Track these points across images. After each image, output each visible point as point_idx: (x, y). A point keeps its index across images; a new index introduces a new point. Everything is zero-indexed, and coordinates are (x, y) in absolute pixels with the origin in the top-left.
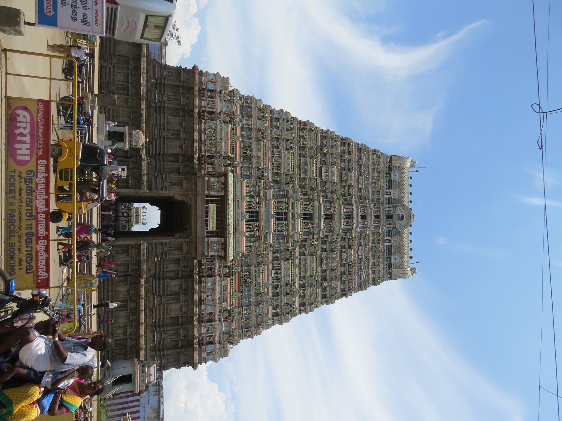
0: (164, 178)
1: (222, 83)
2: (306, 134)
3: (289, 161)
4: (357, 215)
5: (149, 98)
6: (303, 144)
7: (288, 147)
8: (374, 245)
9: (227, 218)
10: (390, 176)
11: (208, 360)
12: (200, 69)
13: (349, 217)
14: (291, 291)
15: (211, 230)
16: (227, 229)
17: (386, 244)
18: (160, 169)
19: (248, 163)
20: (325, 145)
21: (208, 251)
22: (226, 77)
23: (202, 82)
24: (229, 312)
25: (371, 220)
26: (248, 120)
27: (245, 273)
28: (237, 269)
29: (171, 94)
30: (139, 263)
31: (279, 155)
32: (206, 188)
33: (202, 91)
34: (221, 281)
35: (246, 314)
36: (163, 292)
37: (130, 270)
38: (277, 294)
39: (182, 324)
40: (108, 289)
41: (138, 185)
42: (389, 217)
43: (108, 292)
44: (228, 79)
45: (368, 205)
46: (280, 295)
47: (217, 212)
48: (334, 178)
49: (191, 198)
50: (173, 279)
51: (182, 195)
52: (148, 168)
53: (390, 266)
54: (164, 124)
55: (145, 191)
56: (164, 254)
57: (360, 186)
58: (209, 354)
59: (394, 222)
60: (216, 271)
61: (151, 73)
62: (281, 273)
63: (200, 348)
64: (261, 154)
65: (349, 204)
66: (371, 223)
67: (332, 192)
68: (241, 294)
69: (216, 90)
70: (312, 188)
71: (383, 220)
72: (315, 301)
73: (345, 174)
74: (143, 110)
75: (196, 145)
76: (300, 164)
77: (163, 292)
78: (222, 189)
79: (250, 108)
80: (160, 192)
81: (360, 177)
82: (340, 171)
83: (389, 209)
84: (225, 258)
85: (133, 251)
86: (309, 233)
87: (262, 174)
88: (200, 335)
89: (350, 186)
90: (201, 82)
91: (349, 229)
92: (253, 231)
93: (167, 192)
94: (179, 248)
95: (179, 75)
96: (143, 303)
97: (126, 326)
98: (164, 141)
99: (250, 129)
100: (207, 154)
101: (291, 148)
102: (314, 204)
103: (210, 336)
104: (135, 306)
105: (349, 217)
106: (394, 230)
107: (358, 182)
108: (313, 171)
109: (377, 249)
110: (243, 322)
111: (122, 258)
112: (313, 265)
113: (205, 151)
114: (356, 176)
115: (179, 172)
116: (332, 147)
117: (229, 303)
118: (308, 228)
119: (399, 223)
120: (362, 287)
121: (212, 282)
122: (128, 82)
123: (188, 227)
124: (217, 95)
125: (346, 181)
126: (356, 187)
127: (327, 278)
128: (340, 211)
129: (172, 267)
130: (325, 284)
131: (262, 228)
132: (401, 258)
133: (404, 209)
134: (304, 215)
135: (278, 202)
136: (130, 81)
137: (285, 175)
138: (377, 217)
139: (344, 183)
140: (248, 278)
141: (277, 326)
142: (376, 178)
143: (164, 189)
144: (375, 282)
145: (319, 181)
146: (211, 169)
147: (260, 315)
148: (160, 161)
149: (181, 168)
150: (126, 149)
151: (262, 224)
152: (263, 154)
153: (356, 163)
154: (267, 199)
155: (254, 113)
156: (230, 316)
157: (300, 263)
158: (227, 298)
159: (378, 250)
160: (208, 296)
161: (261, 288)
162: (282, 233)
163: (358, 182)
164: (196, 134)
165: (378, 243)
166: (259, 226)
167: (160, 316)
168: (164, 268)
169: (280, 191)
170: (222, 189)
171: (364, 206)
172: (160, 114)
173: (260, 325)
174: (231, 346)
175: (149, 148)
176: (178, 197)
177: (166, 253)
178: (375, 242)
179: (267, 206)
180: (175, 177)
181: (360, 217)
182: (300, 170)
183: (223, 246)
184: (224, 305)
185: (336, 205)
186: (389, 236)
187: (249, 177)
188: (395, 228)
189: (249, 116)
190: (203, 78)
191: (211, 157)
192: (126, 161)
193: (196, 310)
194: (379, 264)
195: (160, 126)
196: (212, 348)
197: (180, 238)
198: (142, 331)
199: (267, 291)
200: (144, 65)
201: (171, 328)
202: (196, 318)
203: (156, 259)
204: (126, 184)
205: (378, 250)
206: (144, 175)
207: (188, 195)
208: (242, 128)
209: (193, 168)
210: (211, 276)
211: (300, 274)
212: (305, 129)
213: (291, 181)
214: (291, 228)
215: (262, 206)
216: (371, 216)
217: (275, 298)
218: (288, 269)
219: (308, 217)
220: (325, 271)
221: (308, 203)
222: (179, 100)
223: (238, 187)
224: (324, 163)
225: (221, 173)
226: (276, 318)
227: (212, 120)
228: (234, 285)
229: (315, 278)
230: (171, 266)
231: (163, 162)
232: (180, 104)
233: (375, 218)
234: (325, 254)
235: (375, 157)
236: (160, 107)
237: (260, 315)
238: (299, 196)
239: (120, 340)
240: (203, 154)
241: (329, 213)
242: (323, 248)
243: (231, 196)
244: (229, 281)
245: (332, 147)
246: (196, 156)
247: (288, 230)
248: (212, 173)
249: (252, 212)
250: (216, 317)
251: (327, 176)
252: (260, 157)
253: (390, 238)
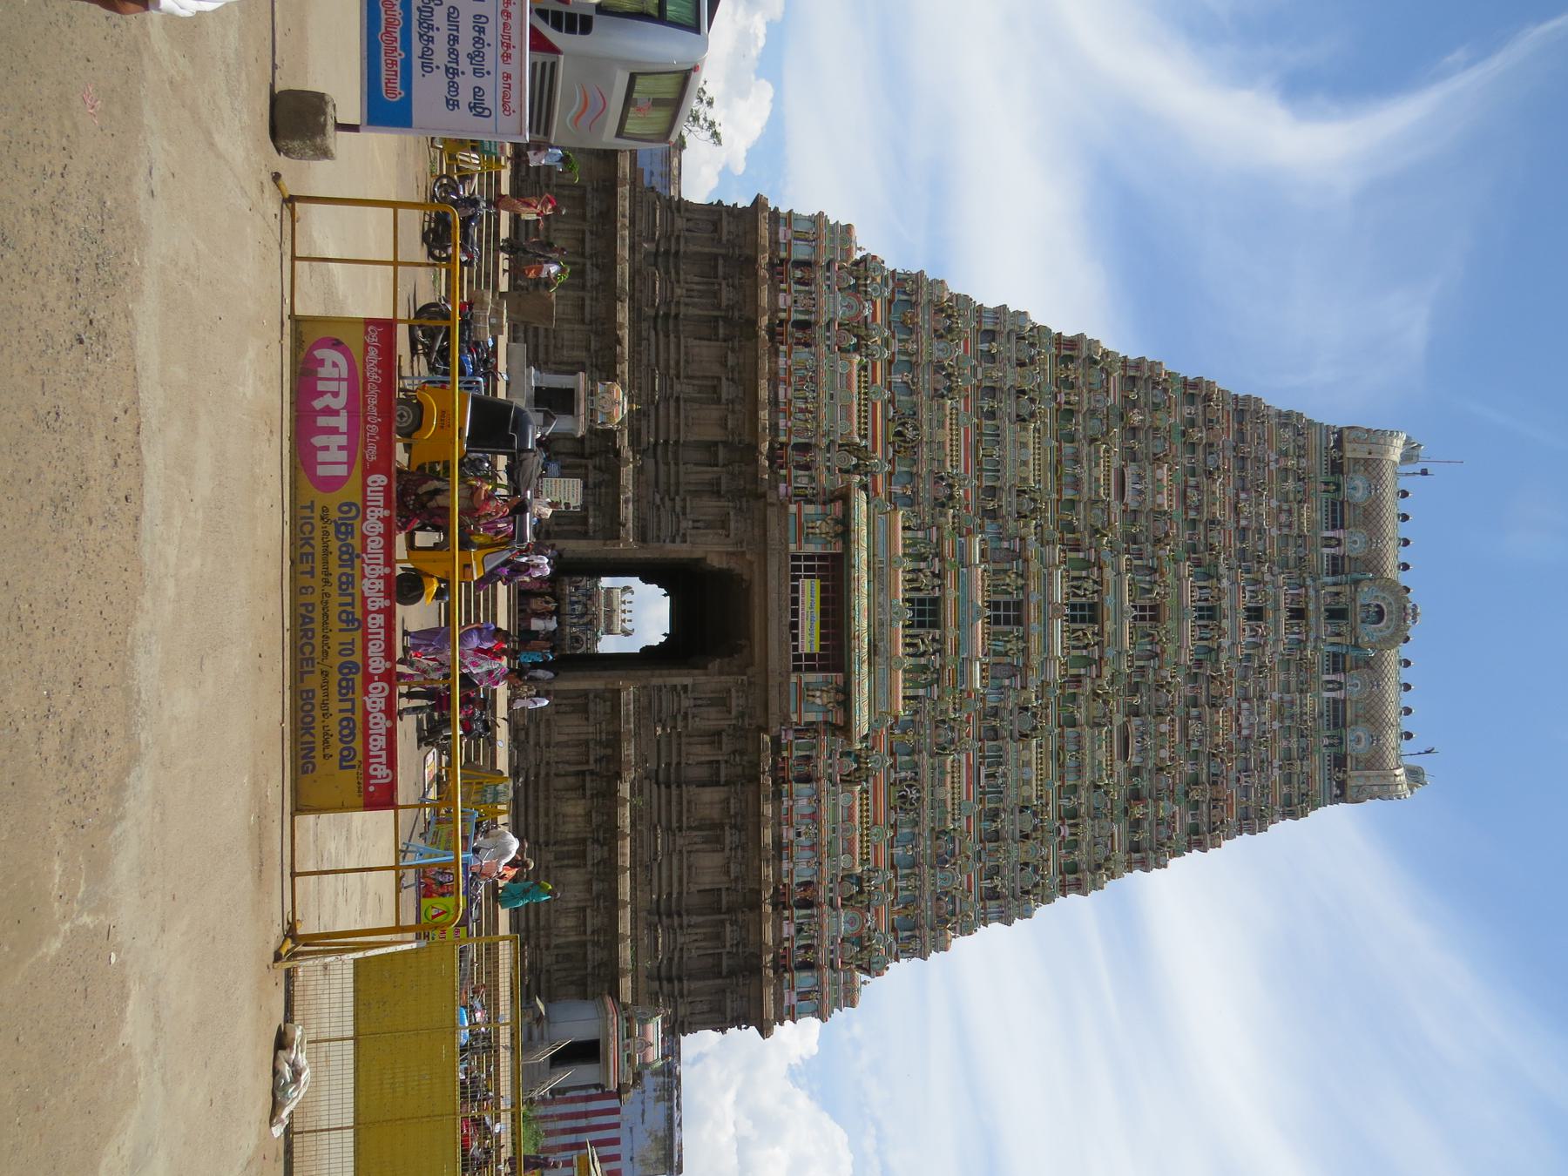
0: (678, 509)
1: (832, 240)
2: (1075, 372)
3: (1027, 455)
4: (1234, 608)
5: (637, 295)
6: (1067, 403)
7: (1024, 412)
8: (1287, 697)
9: (850, 618)
10: (1338, 487)
11: (803, 1014)
12: (772, 206)
13: (1209, 613)
14: (1035, 829)
15: (807, 650)
16: (850, 650)
17: (1326, 694)
18: (668, 483)
19: (908, 462)
20: (1134, 404)
21: (798, 711)
22: (843, 223)
23: (777, 242)
24: (859, 880)
25: (1277, 622)
26: (906, 341)
27: (903, 774)
28: (880, 761)
29: (697, 279)
30: (615, 741)
31: (997, 435)
32: (791, 534)
33: (778, 267)
34: (836, 794)
35: (906, 889)
36: (680, 820)
37: (592, 759)
38: (996, 836)
39: (729, 911)
40: (537, 809)
41: (612, 530)
42: (1336, 614)
43: (537, 816)
44: (849, 228)
45: (1267, 578)
46: (1005, 839)
47: (823, 601)
48: (1163, 500)
49: (751, 563)
50: (702, 784)
51: (728, 553)
52: (637, 483)
53: (1339, 762)
54: (678, 363)
55: (628, 545)
56: (679, 718)
57: (1243, 523)
58: (803, 996)
59: (1354, 629)
60: (821, 764)
61: (642, 225)
62: (1004, 775)
63: (780, 978)
64: (945, 435)
65: (1209, 576)
66: (1277, 632)
67: (1158, 541)
68: (890, 834)
69: (816, 263)
70: (1097, 531)
72: (1107, 859)
73: (1197, 487)
74: (621, 326)
75: (764, 415)
76: (1059, 462)
77: (680, 820)
78: (837, 535)
79: (914, 305)
80: (669, 546)
81: (1243, 496)
82: (1181, 479)
83: (1334, 589)
84: (845, 729)
85: (599, 708)
86: (1088, 662)
87: (948, 492)
88: (779, 941)
89: (1212, 522)
90: (775, 242)
91: (1211, 650)
92: (923, 654)
93: (684, 546)
94: (721, 702)
95: (716, 225)
96: (625, 847)
97: (584, 909)
98: (678, 409)
99: (912, 366)
100: (794, 440)
101: (1032, 415)
102: (1101, 575)
103: (808, 947)
104: (606, 855)
105: (1209, 613)
107: (1237, 511)
108: (1097, 480)
109: (1297, 709)
110: (898, 912)
111: (570, 727)
112: (1102, 755)
113: (789, 432)
114: (1230, 491)
115: (718, 492)
116: (1156, 407)
117: (857, 856)
118: (1085, 647)
120: (1253, 821)
121: (809, 797)
122: (583, 255)
123: (743, 642)
124: (820, 274)
125: (1198, 509)
126: (1231, 525)
127: (1145, 793)
128: (1180, 596)
129: (703, 752)
130: (1138, 811)
131: (949, 648)
132: (1376, 737)
134: (1073, 607)
135: (996, 572)
136: (588, 250)
137: (1014, 493)
138: (1298, 614)
139: (1192, 514)
140: (910, 786)
141: (996, 927)
142: (1291, 497)
143: (678, 539)
144: (1294, 808)
145: (1116, 508)
146: (805, 480)
147: (946, 894)
148: (667, 464)
149: (723, 480)
150: (580, 434)
151: (951, 633)
152: (949, 434)
153: (1230, 454)
154: (964, 562)
155: (924, 319)
156: (861, 892)
157: (1061, 748)
158: (851, 842)
159: (1302, 714)
160: (799, 835)
161: (949, 817)
162: (1008, 660)
163: (1237, 511)
164: (764, 384)
165: (1301, 691)
166: (941, 641)
167: (670, 885)
168: (679, 755)
169: (1001, 540)
170: (837, 535)
171: (1256, 582)
172: (667, 336)
173: (947, 922)
174: (864, 977)
175: (639, 430)
176: (716, 562)
177: (686, 714)
178: (1293, 686)
179: (963, 584)
180: (709, 506)
181: (1242, 614)
182: (1059, 479)
183: (841, 697)
184: (844, 860)
185: (1169, 578)
186: (1335, 671)
187: (911, 501)
188: (1356, 646)
189: (910, 329)
190: (782, 230)
191: (804, 448)
192: (580, 466)
193: (768, 872)
194: (1304, 754)
195: (667, 367)
196: (812, 981)
197: (721, 673)
198: (625, 926)
199: (965, 826)
200: (624, 205)
201: (701, 919)
202: (767, 894)
203: (659, 730)
204: (579, 528)
205: (1302, 714)
206: (626, 501)
207: (743, 553)
208: (890, 362)
209: (755, 478)
210: (807, 779)
211: (1062, 778)
212: (1071, 359)
213: (1033, 511)
214: (1034, 644)
215: (948, 582)
216: (1277, 609)
217: (989, 846)
218: (1028, 764)
219: (1085, 613)
220: (1136, 771)
221: (1084, 574)
222: (716, 294)
223: (881, 528)
224: (1132, 456)
225: (832, 492)
226: (993, 903)
227: (807, 345)
228: (871, 807)
229: (1106, 793)
230: (698, 749)
231: (677, 464)
232: (719, 307)
233: (1291, 617)
234: (1136, 721)
235: (1288, 434)
236: (667, 315)
237: (946, 894)
238: (1056, 552)
239: (569, 944)
240: (783, 439)
241: (1148, 603)
242: (1131, 705)
243: (861, 557)
244: (857, 796)
245: (1156, 407)
246: (765, 447)
247: (1025, 651)
248: (810, 491)
249: (921, 601)
250: (823, 894)
251: (1140, 492)
252: (942, 445)
253: (1340, 677)
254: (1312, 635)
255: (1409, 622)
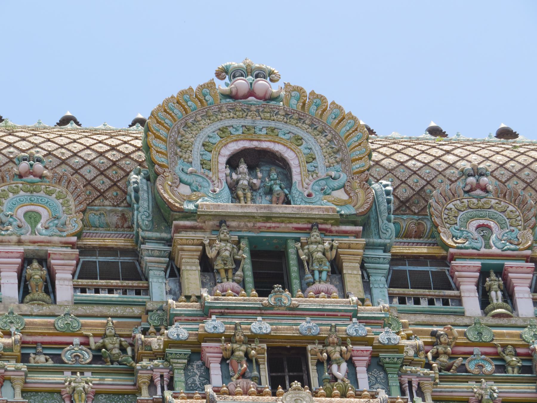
42: (270, 268)
59: (313, 224)
71: (308, 308)
83: (192, 275)
106: (388, 230)
119: (316, 191)
133: (181, 148)
186: (445, 282)
188: (366, 221)
254: (353, 328)
255: (275, 88)
